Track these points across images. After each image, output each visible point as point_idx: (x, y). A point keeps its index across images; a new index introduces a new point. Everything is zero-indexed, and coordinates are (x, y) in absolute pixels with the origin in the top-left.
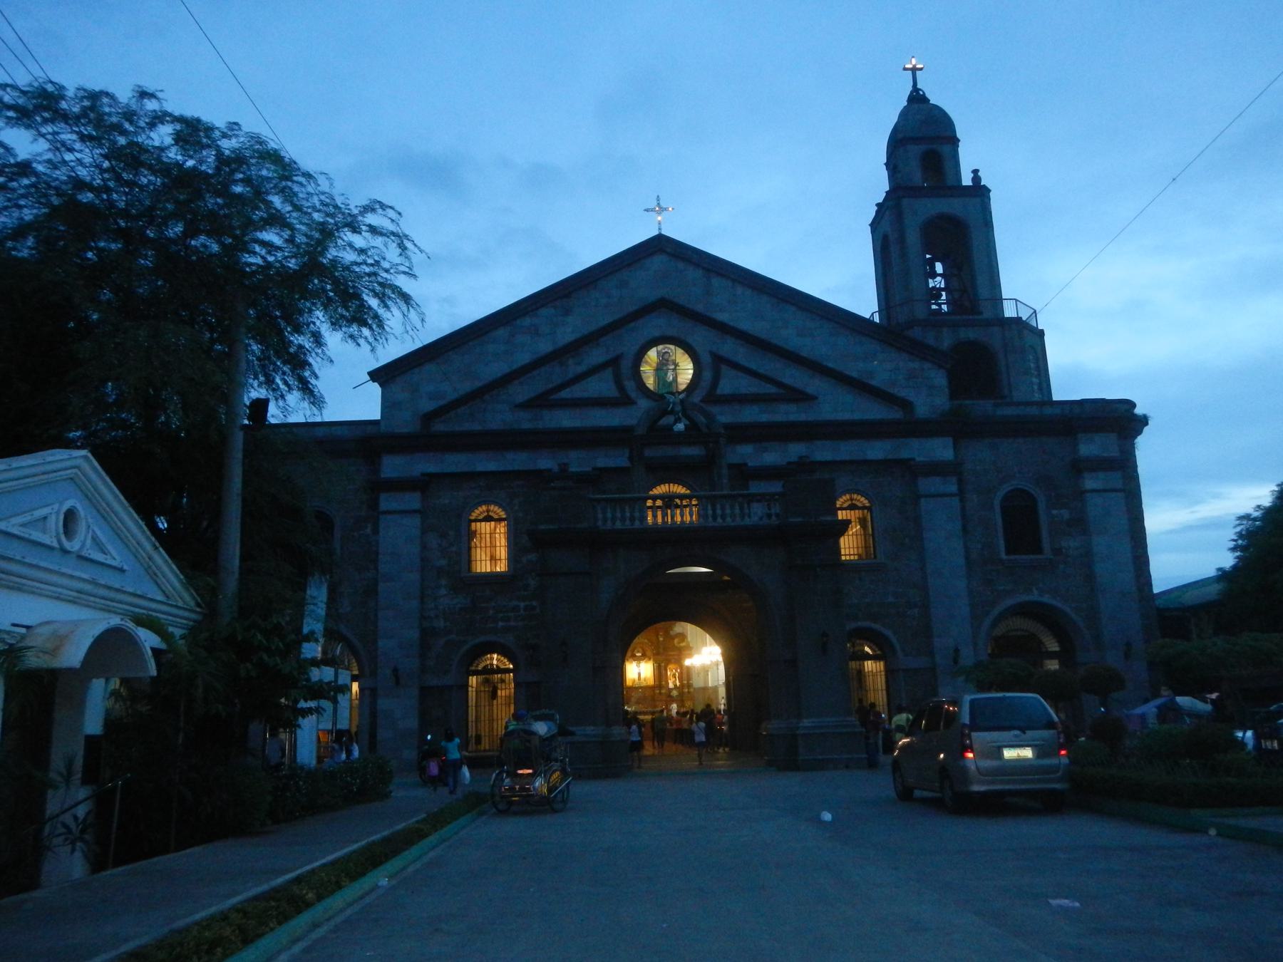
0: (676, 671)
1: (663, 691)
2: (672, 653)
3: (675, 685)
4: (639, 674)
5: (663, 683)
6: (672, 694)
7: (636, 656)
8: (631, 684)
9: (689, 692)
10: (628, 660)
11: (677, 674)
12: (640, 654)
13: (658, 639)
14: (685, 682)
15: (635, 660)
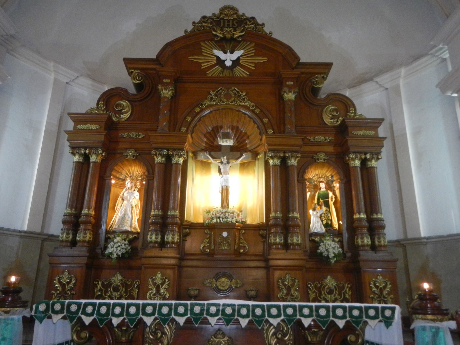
0: (329, 187)
1: (296, 239)
2: (320, 138)
3: (328, 226)
4: (225, 192)
5: (296, 214)
6: (322, 249)
7: (219, 148)
8: (201, 221)
9: (373, 247)
10: (195, 154)
11: (330, 194)
12: (230, 142)
13: (281, 98)
14: (363, 216)
15: (214, 158)
